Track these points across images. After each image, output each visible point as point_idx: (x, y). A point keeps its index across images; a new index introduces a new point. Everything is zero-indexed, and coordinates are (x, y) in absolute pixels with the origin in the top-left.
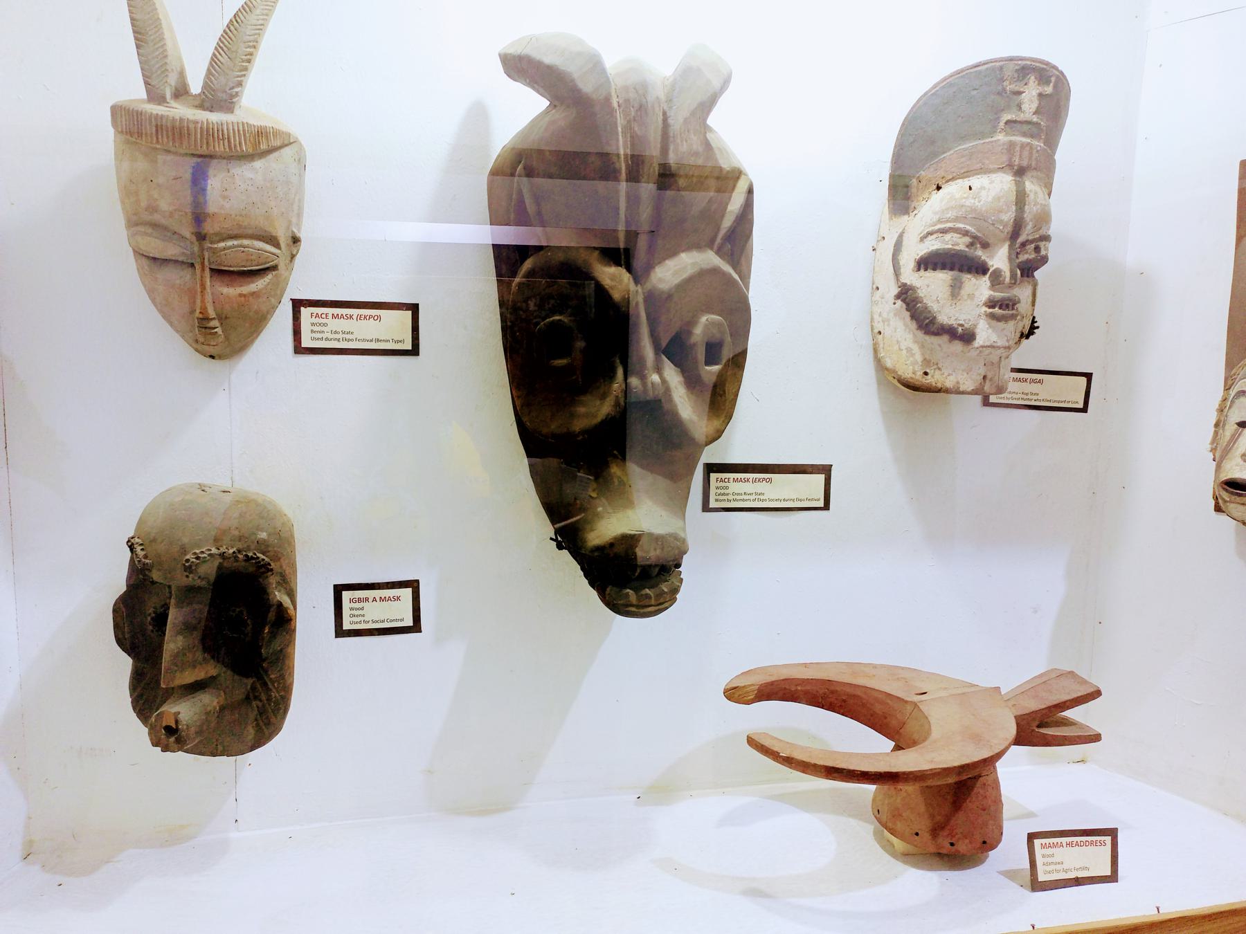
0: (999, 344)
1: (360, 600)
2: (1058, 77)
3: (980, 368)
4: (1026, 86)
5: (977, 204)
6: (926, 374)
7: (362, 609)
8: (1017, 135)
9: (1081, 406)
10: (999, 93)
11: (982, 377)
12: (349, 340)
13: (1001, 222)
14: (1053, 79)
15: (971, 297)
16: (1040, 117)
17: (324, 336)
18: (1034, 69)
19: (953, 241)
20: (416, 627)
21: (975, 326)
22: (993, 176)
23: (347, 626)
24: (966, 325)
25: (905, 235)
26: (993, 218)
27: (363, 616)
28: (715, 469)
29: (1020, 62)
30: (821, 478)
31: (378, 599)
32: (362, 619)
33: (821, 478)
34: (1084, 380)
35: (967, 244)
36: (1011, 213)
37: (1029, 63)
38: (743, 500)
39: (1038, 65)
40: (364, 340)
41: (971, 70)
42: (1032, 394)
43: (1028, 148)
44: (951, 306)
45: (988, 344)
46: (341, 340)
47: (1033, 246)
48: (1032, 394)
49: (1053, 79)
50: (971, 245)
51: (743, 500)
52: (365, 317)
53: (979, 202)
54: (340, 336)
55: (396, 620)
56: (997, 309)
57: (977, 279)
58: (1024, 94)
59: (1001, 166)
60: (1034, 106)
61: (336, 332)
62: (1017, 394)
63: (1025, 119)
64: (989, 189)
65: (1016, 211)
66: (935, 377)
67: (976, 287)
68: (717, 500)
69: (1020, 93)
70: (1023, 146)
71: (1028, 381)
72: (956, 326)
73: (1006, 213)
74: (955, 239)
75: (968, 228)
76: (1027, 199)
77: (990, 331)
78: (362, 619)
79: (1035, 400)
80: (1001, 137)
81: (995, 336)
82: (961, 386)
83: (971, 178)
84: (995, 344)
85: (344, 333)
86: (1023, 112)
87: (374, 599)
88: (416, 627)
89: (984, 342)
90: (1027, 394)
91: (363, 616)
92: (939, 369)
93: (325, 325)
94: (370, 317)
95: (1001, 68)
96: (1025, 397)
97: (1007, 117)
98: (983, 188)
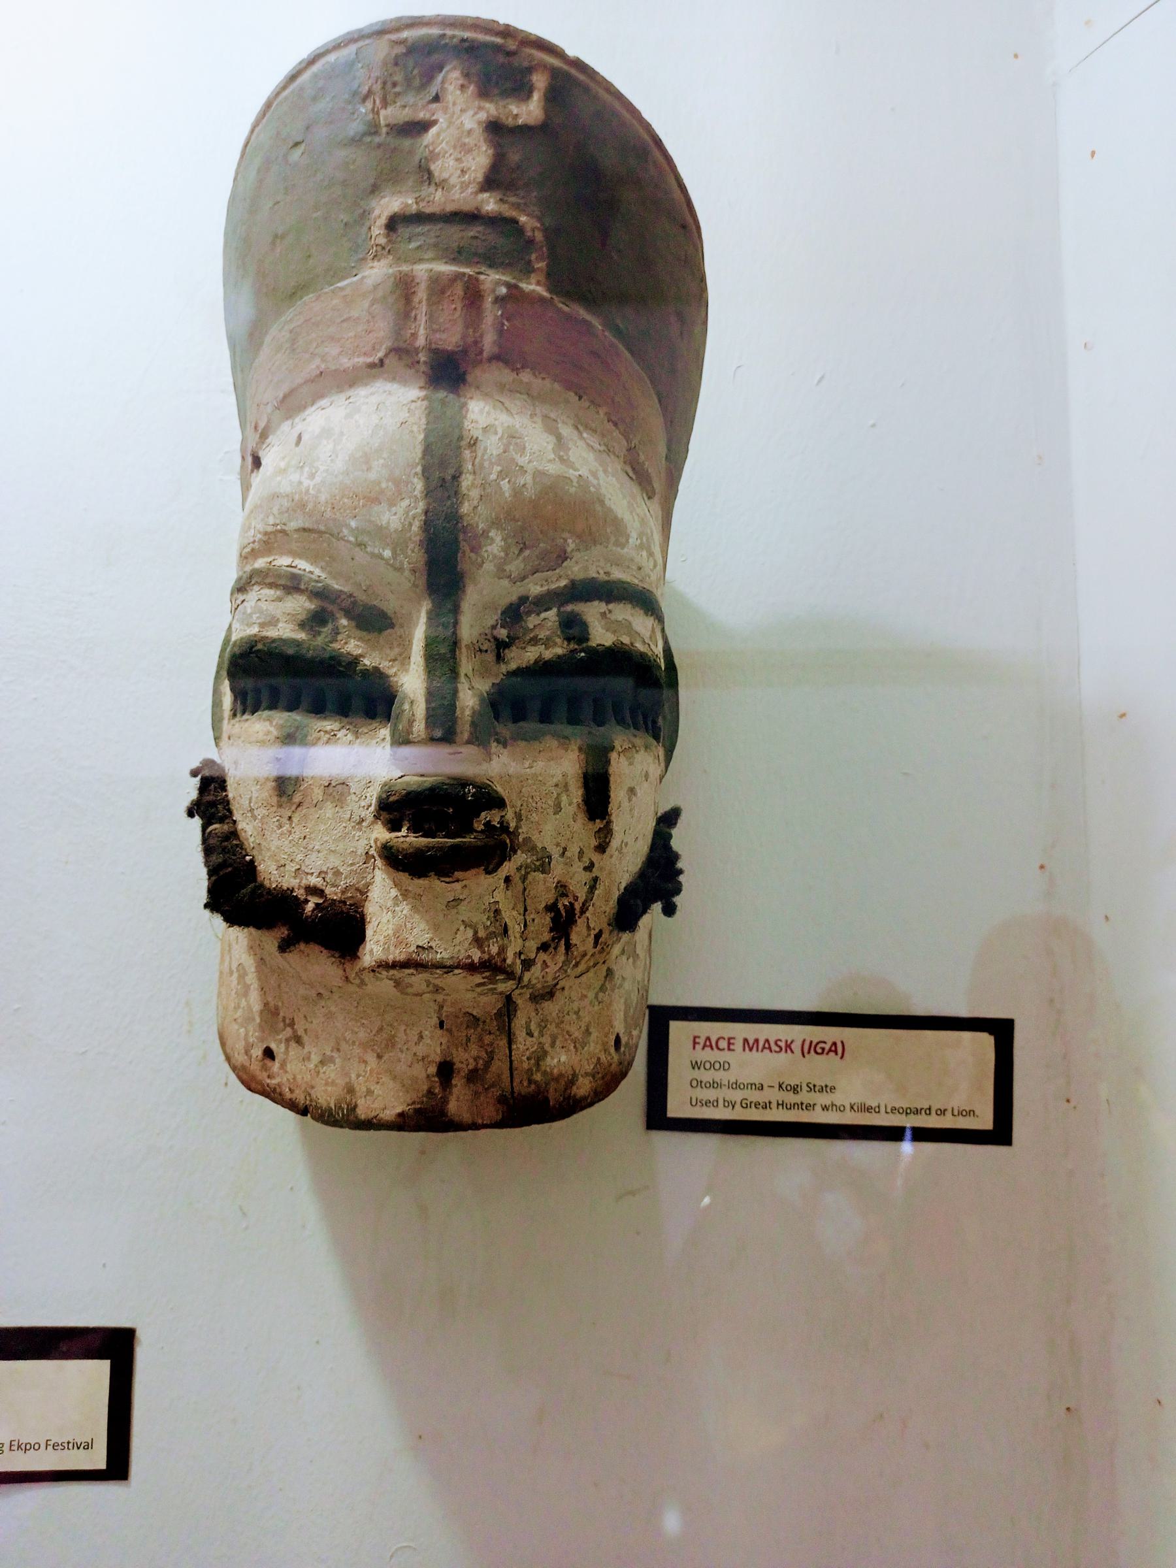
0: (443, 954)
2: (555, 73)
3: (421, 1037)
4: (434, 106)
5: (306, 483)
6: (269, 1054)
9: (985, 1121)
11: (433, 1070)
13: (380, 532)
14: (540, 81)
16: (513, 199)
18: (469, 50)
21: (363, 892)
24: (328, 891)
26: (353, 524)
29: (405, 34)
30: (99, 1370)
33: (99, 1370)
35: (303, 617)
36: (406, 503)
37: (435, 31)
39: (467, 34)
42: (812, 1088)
44: (280, 827)
45: (397, 954)
47: (552, 615)
48: (812, 1088)
49: (540, 81)
50: (316, 620)
53: (312, 476)
56: (404, 832)
58: (433, 131)
59: (375, 359)
60: (480, 161)
62: (762, 1088)
63: (450, 208)
64: (342, 434)
65: (428, 493)
66: (289, 1067)
69: (419, 127)
71: (796, 1047)
72: (300, 893)
73: (392, 504)
74: (264, 605)
75: (303, 565)
76: (467, 454)
77: (405, 908)
79: (825, 1108)
81: (423, 926)
82: (361, 1102)
84: (425, 957)
86: (442, 184)
89: (386, 950)
90: (795, 1089)
92: (298, 1040)
96: (791, 1098)
98: (326, 432)
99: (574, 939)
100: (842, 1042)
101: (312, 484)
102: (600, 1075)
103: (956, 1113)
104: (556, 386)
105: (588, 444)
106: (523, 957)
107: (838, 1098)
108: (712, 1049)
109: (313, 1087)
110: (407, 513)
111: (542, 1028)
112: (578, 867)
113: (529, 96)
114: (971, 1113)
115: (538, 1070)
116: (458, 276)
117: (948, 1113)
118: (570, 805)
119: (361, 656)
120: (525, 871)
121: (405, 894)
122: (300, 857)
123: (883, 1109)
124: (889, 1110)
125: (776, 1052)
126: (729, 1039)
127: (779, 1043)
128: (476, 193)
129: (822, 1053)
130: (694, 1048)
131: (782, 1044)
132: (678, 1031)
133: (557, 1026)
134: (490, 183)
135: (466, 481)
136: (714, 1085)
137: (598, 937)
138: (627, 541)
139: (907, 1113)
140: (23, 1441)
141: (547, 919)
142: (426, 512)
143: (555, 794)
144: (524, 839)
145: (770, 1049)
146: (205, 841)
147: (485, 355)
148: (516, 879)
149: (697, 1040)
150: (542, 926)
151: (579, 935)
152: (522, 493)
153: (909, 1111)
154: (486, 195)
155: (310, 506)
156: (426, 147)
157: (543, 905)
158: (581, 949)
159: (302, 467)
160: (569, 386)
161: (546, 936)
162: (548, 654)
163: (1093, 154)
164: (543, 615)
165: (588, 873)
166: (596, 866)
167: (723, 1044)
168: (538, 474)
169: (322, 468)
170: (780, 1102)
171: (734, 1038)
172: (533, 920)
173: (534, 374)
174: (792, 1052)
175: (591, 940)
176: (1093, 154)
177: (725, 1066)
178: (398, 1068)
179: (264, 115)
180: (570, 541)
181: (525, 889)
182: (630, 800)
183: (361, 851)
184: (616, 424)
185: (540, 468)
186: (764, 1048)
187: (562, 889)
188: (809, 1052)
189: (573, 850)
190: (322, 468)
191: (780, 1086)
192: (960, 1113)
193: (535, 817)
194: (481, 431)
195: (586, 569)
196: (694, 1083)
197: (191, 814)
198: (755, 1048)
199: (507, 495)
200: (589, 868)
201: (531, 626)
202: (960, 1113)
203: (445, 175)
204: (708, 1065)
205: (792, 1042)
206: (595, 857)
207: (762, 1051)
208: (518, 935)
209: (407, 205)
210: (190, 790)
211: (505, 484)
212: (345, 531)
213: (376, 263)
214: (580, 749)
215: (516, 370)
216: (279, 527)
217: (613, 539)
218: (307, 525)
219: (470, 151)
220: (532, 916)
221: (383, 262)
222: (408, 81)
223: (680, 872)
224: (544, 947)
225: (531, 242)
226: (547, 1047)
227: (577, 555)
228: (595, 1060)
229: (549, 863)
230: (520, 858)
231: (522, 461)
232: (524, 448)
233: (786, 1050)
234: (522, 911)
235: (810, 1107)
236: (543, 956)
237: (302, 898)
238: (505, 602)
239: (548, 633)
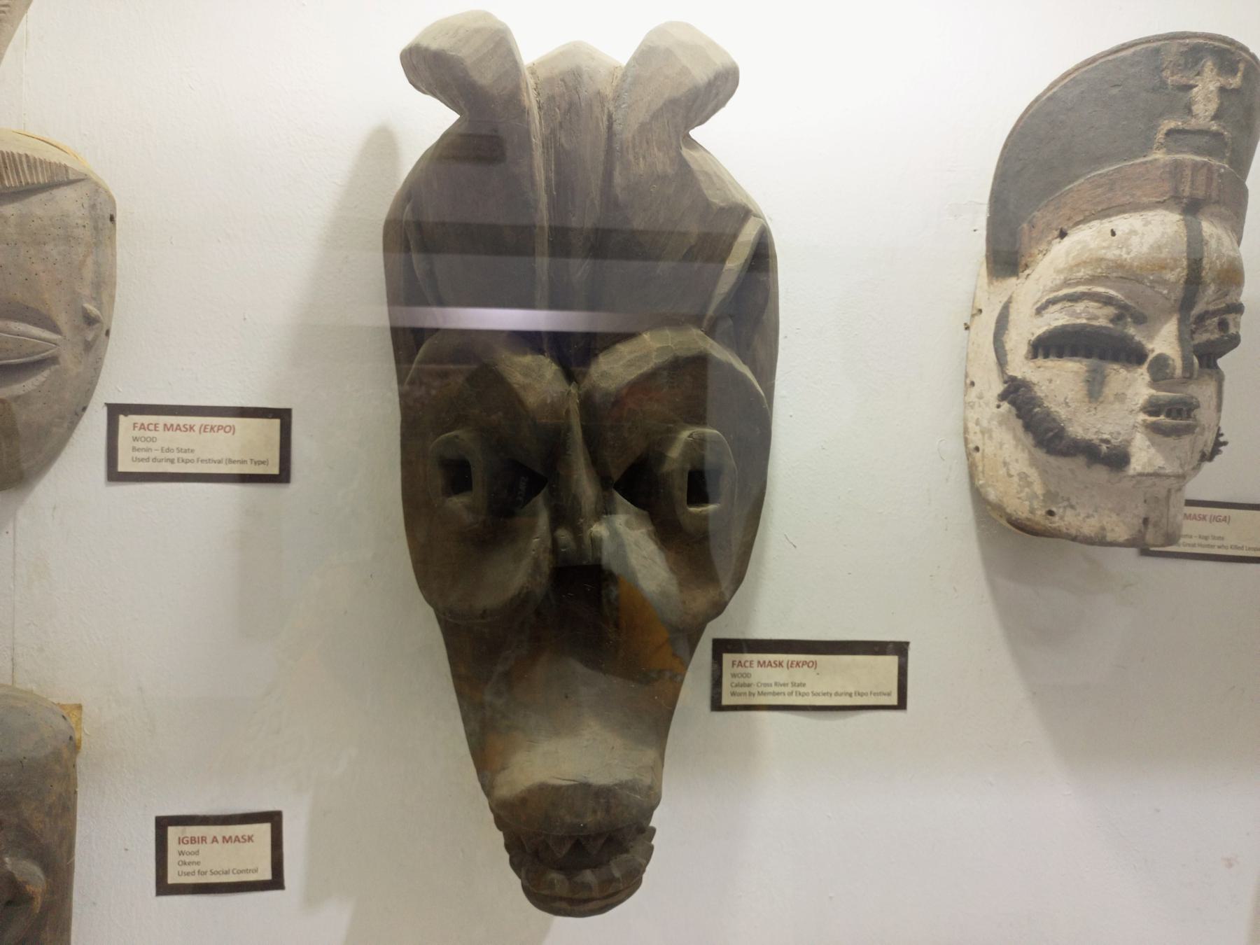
0: (1168, 471)
1: (193, 840)
2: (1247, 62)
3: (1137, 507)
4: (1198, 77)
5: (1125, 256)
6: (1051, 513)
7: (197, 853)
8: (1184, 152)
10: (1154, 90)
11: (1141, 521)
12: (186, 461)
13: (1164, 282)
14: (1242, 66)
15: (1120, 397)
17: (152, 455)
19: (1089, 312)
20: (276, 882)
21: (1128, 442)
22: (1150, 215)
23: (173, 878)
24: (1113, 441)
25: (1011, 305)
26: (1151, 278)
27: (198, 863)
28: (729, 647)
29: (1187, 41)
30: (892, 661)
31: (220, 839)
32: (196, 868)
36: (1179, 270)
38: (774, 694)
39: (1216, 44)
40: (209, 461)
41: (1110, 58)
42: (1214, 538)
43: (1205, 170)
44: (1089, 411)
45: (1149, 470)
46: (176, 461)
47: (1216, 320)
48: (1214, 538)
50: (1117, 319)
51: (774, 694)
52: (212, 428)
53: (1128, 253)
54: (174, 455)
55: (247, 871)
56: (1162, 417)
58: (1195, 90)
59: (1161, 200)
60: (1213, 107)
61: (169, 450)
62: (1191, 537)
63: (1197, 128)
64: (1143, 234)
65: (1189, 266)
66: (1066, 519)
67: (1127, 383)
68: (733, 694)
70: (1196, 167)
71: (1208, 518)
72: (1097, 442)
73: (1172, 270)
74: (1091, 310)
75: (1112, 292)
76: (1205, 248)
77: (1153, 450)
78: (196, 868)
79: (1219, 547)
80: (1159, 156)
81: (1161, 458)
83: (1113, 219)
84: (1162, 471)
85: (180, 450)
86: (1195, 116)
87: (215, 840)
88: (276, 882)
90: (1206, 538)
91: (198, 863)
92: (1072, 507)
93: (153, 440)
94: (220, 428)
95: (1157, 51)
96: (1204, 542)
97: (1169, 124)
98: (1133, 232)
101: (1129, 256)
107: (1225, 543)
109: (1082, 528)
110: (1178, 275)
113: (1236, 74)
116: (1205, 164)
119: (1135, 335)
121: (1153, 444)
122: (1099, 426)
128: (1209, 121)
134: (1216, 117)
135: (1205, 261)
140: (860, 691)
142: (1187, 275)
154: (1213, 122)
155: (1127, 267)
156: (1191, 98)
159: (1121, 248)
169: (1134, 250)
179: (1089, 64)
183: (1131, 424)
190: (1134, 250)
201: (1206, 324)
203: (1198, 112)
209: (1178, 125)
211: (1218, 261)
212: (1146, 281)
213: (1157, 152)
216: (1104, 274)
218: (1124, 276)
219: (1210, 101)
221: (1162, 151)
222: (1186, 64)
225: (1226, 144)
235: (1213, 546)
237: (1098, 444)
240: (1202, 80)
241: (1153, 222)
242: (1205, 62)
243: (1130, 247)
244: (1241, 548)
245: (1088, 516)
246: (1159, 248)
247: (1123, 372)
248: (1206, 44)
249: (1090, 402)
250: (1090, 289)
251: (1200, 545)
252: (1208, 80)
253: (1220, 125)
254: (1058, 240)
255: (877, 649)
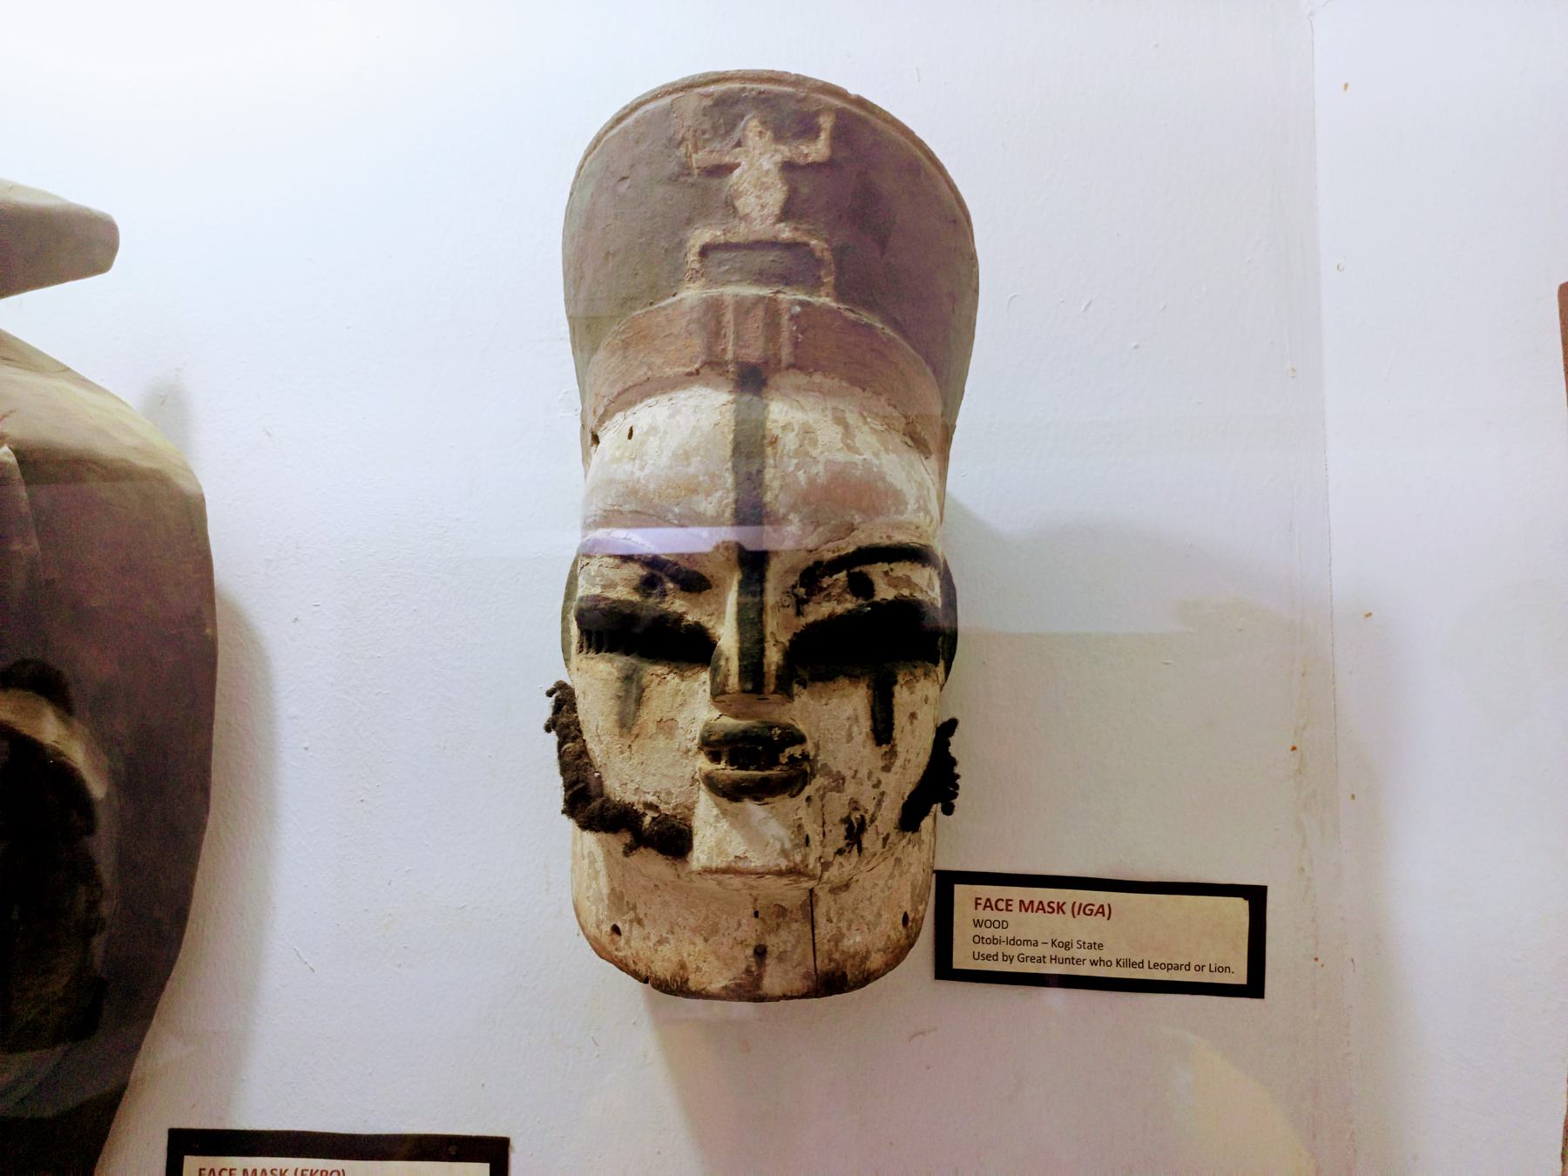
0: (756, 862)
2: (840, 114)
3: (739, 924)
4: (738, 150)
5: (638, 473)
6: (616, 930)
10: (673, 179)
11: (750, 952)
15: (666, 726)
16: (805, 226)
18: (764, 102)
19: (603, 575)
21: (690, 808)
22: (681, 396)
24: (662, 807)
26: (677, 510)
29: (712, 88)
34: (1240, 906)
35: (636, 582)
37: (736, 86)
42: (1082, 945)
43: (760, 312)
44: (622, 753)
45: (719, 862)
48: (1082, 945)
49: (826, 122)
50: (648, 585)
53: (642, 468)
56: (722, 765)
57: (683, 678)
58: (737, 172)
59: (692, 369)
60: (775, 197)
62: (1036, 944)
63: (752, 238)
64: (666, 432)
65: (737, 485)
66: (632, 944)
67: (679, 699)
69: (723, 170)
70: (744, 308)
71: (1067, 908)
72: (639, 808)
73: (708, 494)
74: (605, 571)
77: (724, 825)
79: (1093, 963)
80: (692, 293)
81: (739, 839)
82: (692, 977)
83: (637, 407)
84: (741, 865)
86: (745, 218)
90: (1067, 946)
92: (640, 922)
95: (667, 112)
96: (1062, 953)
97: (703, 235)
98: (653, 430)
99: (865, 843)
100: (1109, 905)
101: (642, 474)
102: (890, 950)
103: (1213, 969)
104: (844, 384)
105: (871, 428)
106: (822, 860)
107: (1105, 955)
108: (992, 909)
109: (652, 962)
110: (720, 502)
111: (840, 915)
112: (868, 785)
113: (817, 136)
114: (1226, 969)
115: (837, 950)
116: (760, 299)
117: (1206, 969)
118: (860, 734)
119: (685, 613)
120: (824, 791)
121: (724, 813)
122: (638, 779)
123: (1146, 965)
124: (1152, 966)
125: (1048, 912)
126: (1007, 900)
127: (1051, 904)
128: (774, 224)
129: (1091, 915)
130: (976, 908)
131: (1055, 906)
132: (961, 892)
133: (853, 911)
134: (787, 213)
135: (769, 474)
136: (994, 941)
137: (885, 839)
138: (906, 508)
139: (1168, 969)
141: (842, 830)
142: (736, 501)
143: (847, 726)
144: (822, 765)
145: (1043, 909)
146: (560, 757)
147: (783, 364)
148: (816, 798)
149: (979, 901)
150: (838, 835)
151: (868, 839)
152: (815, 480)
153: (1170, 967)
154: (782, 225)
155: (641, 494)
156: (731, 186)
157: (839, 818)
158: (872, 851)
159: (634, 459)
160: (854, 381)
161: (842, 843)
162: (839, 609)
163: (1346, 86)
164: (835, 577)
165: (876, 790)
166: (883, 782)
167: (1002, 905)
168: (828, 462)
170: (1053, 957)
171: (1011, 900)
172: (831, 831)
173: (825, 375)
174: (1064, 913)
175: (880, 842)
176: (1346, 86)
177: (1003, 924)
178: (722, 950)
179: (595, 148)
180: (856, 516)
181: (823, 806)
182: (912, 723)
183: (688, 776)
184: (895, 407)
185: (830, 457)
186: (1038, 909)
187: (855, 805)
188: (1079, 914)
189: (863, 773)
191: (1053, 943)
192: (1217, 969)
193: (831, 746)
194: (780, 430)
195: (871, 536)
196: (977, 939)
197: (548, 729)
198: (1030, 908)
199: (803, 483)
200: (877, 785)
201: (825, 586)
202: (1217, 969)
203: (748, 210)
204: (988, 924)
205: (1064, 903)
206: (883, 776)
207: (1036, 912)
208: (818, 844)
209: (717, 236)
210: (546, 708)
211: (801, 475)
212: (670, 516)
213: (691, 285)
214: (868, 687)
215: (810, 374)
216: (616, 507)
217: (893, 509)
218: (639, 509)
219: (767, 189)
220: (829, 828)
221: (698, 284)
222: (715, 128)
223: (958, 776)
224: (840, 852)
225: (819, 263)
226: (844, 930)
227: (862, 526)
228: (885, 938)
229: (844, 783)
230: (819, 781)
231: (815, 453)
232: (817, 441)
233: (1058, 912)
234: (821, 824)
235: (1079, 962)
236: (839, 859)
237: (641, 811)
238: (803, 566)
239: (839, 591)
240: (747, 152)
241: (683, 409)
242: (747, 122)
243: (645, 458)
244: (1141, 965)
245: (660, 942)
246: (687, 456)
247: (673, 680)
248: (743, 90)
249: (621, 736)
250: (609, 534)
251: (1054, 959)
252: (758, 152)
253: (796, 229)
254: (593, 448)
255: (452, 1150)
